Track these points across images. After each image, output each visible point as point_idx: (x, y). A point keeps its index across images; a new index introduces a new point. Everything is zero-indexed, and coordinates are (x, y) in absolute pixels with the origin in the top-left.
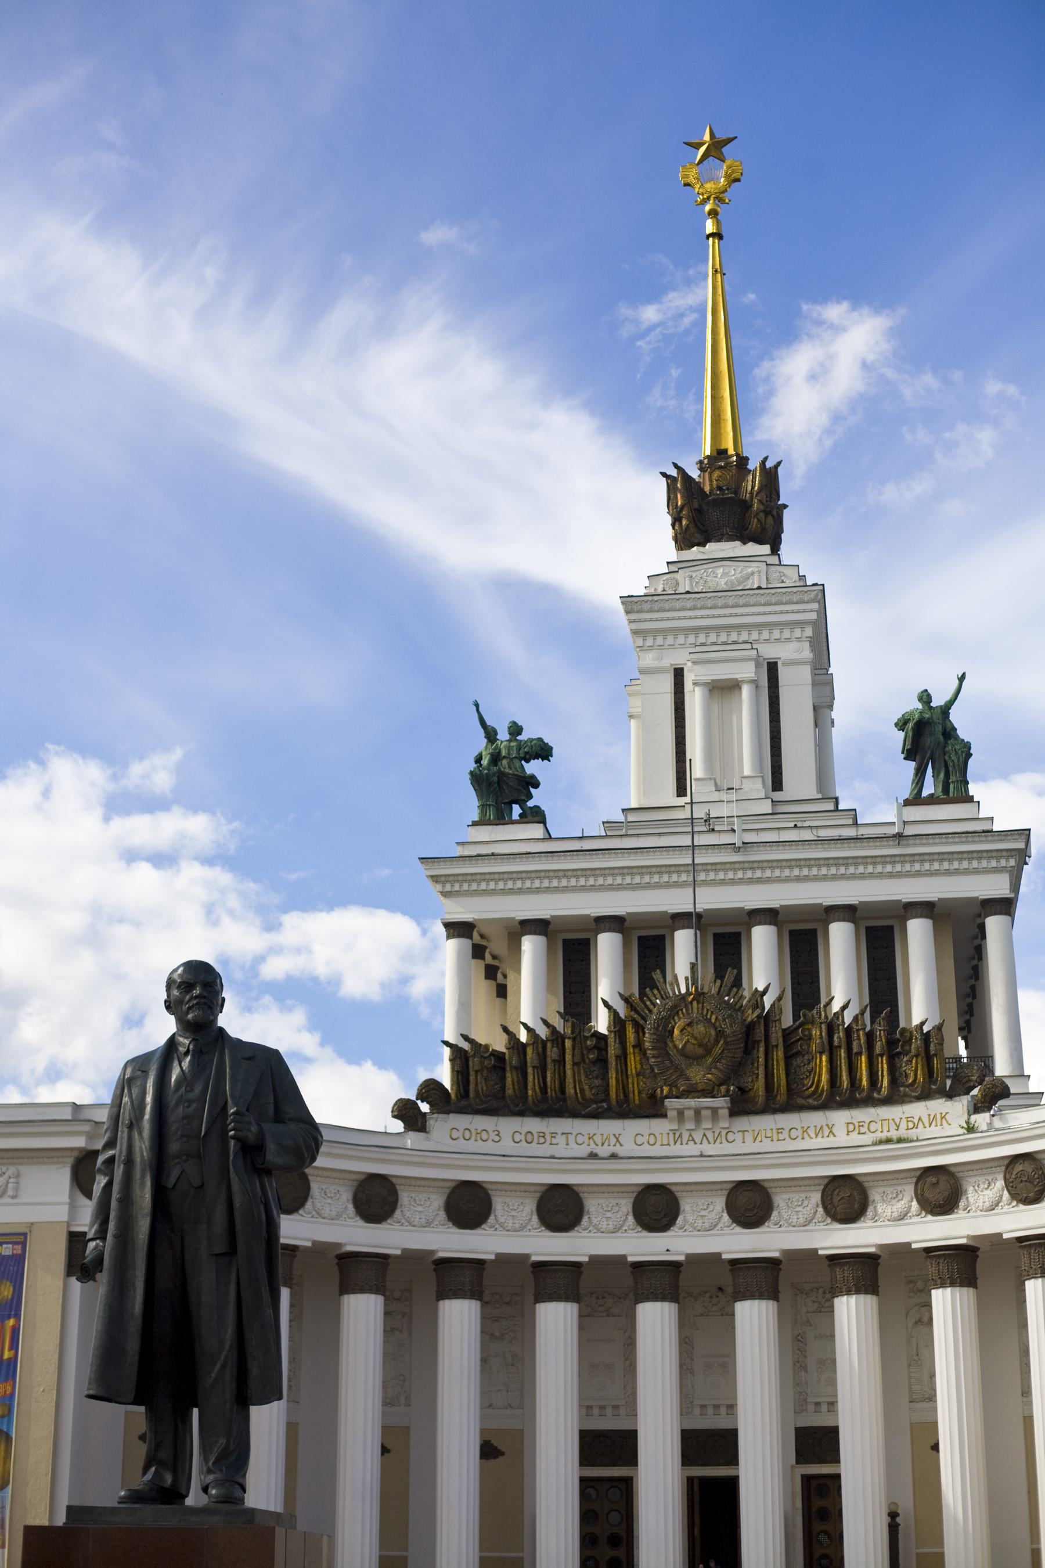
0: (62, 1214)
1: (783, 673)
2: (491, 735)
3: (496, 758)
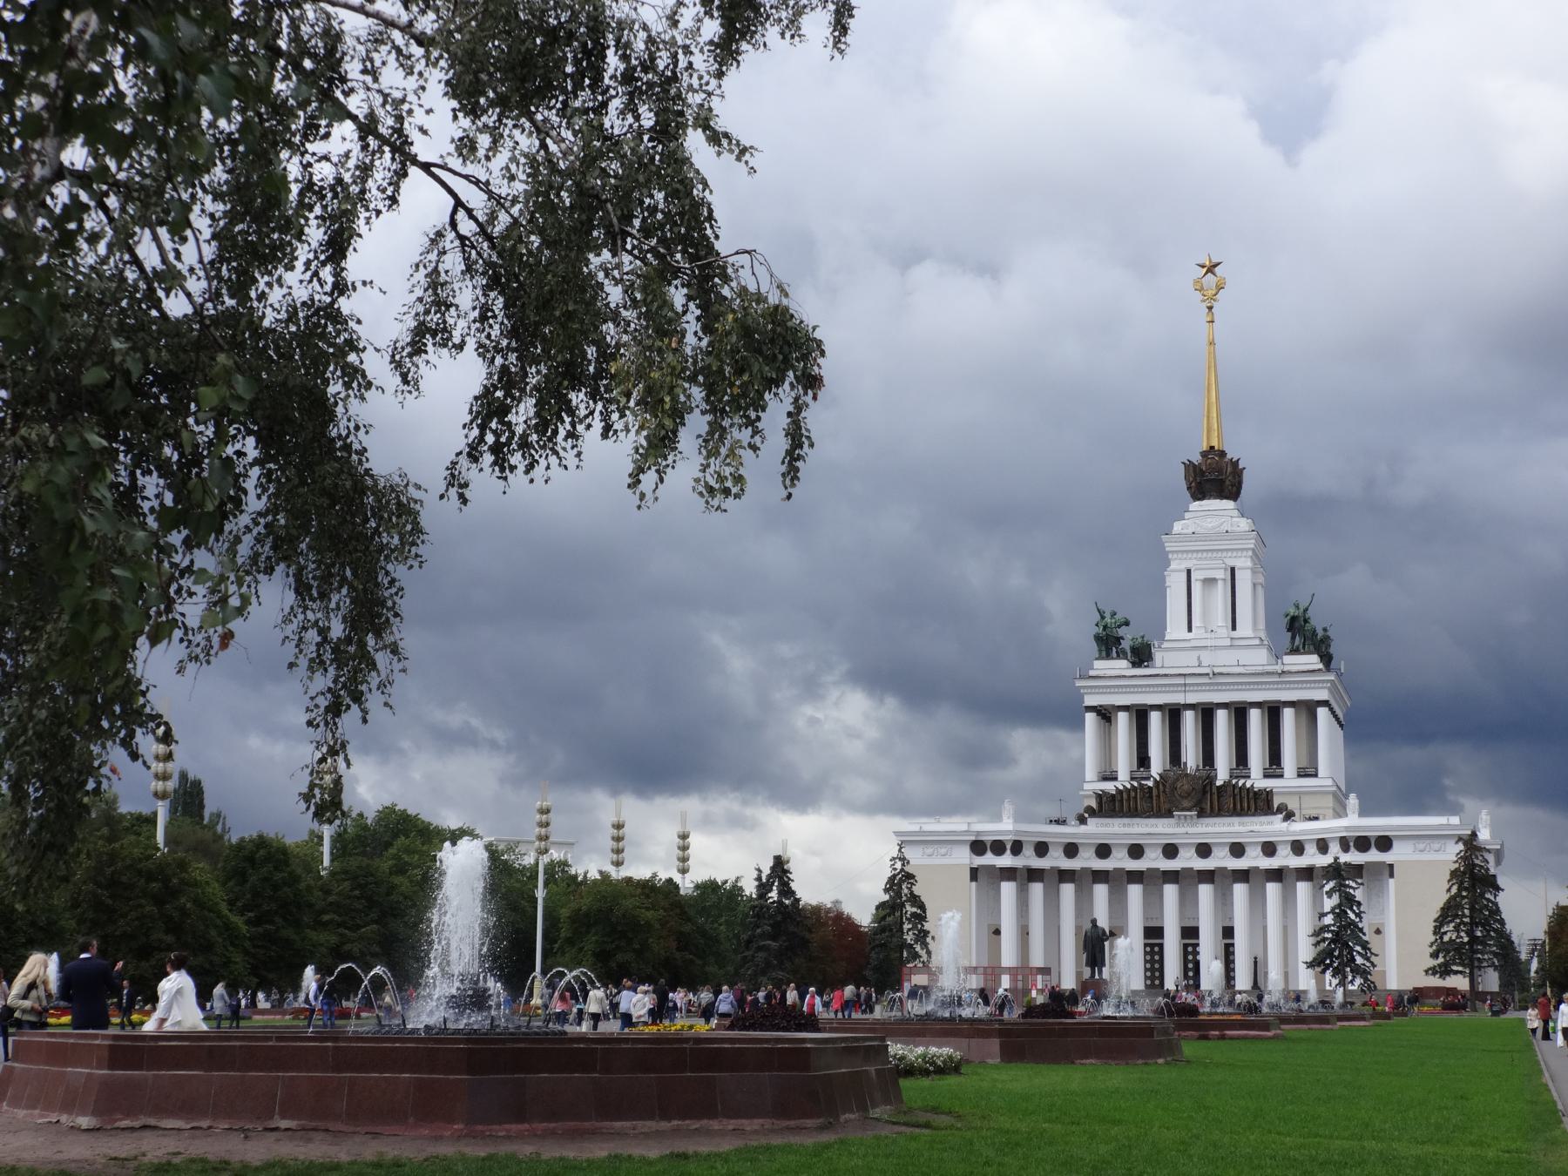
0: (967, 861)
3: (1105, 627)
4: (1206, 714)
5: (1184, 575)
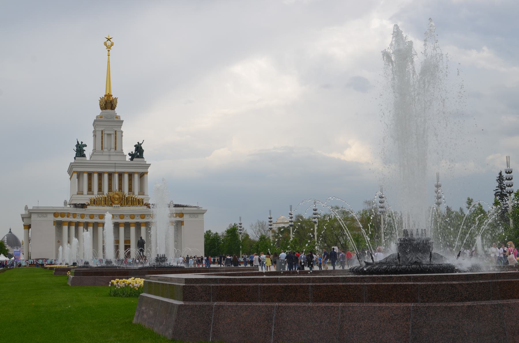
0: (53, 219)
1: (117, 133)
2: (78, 142)
3: (79, 147)
4: (121, 175)
5: (101, 132)
